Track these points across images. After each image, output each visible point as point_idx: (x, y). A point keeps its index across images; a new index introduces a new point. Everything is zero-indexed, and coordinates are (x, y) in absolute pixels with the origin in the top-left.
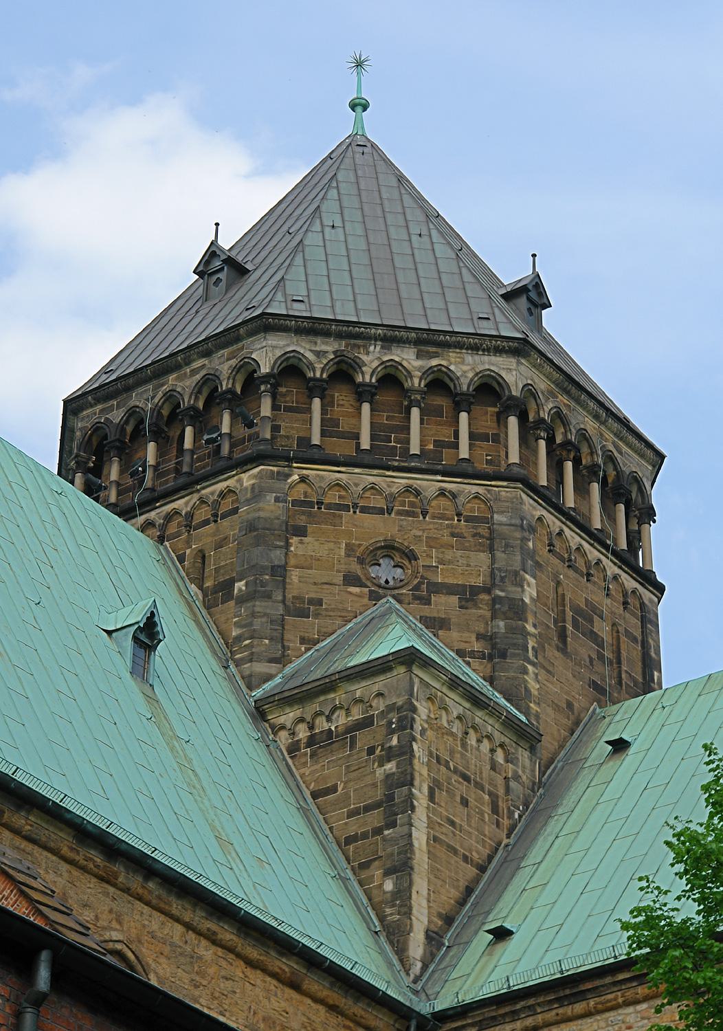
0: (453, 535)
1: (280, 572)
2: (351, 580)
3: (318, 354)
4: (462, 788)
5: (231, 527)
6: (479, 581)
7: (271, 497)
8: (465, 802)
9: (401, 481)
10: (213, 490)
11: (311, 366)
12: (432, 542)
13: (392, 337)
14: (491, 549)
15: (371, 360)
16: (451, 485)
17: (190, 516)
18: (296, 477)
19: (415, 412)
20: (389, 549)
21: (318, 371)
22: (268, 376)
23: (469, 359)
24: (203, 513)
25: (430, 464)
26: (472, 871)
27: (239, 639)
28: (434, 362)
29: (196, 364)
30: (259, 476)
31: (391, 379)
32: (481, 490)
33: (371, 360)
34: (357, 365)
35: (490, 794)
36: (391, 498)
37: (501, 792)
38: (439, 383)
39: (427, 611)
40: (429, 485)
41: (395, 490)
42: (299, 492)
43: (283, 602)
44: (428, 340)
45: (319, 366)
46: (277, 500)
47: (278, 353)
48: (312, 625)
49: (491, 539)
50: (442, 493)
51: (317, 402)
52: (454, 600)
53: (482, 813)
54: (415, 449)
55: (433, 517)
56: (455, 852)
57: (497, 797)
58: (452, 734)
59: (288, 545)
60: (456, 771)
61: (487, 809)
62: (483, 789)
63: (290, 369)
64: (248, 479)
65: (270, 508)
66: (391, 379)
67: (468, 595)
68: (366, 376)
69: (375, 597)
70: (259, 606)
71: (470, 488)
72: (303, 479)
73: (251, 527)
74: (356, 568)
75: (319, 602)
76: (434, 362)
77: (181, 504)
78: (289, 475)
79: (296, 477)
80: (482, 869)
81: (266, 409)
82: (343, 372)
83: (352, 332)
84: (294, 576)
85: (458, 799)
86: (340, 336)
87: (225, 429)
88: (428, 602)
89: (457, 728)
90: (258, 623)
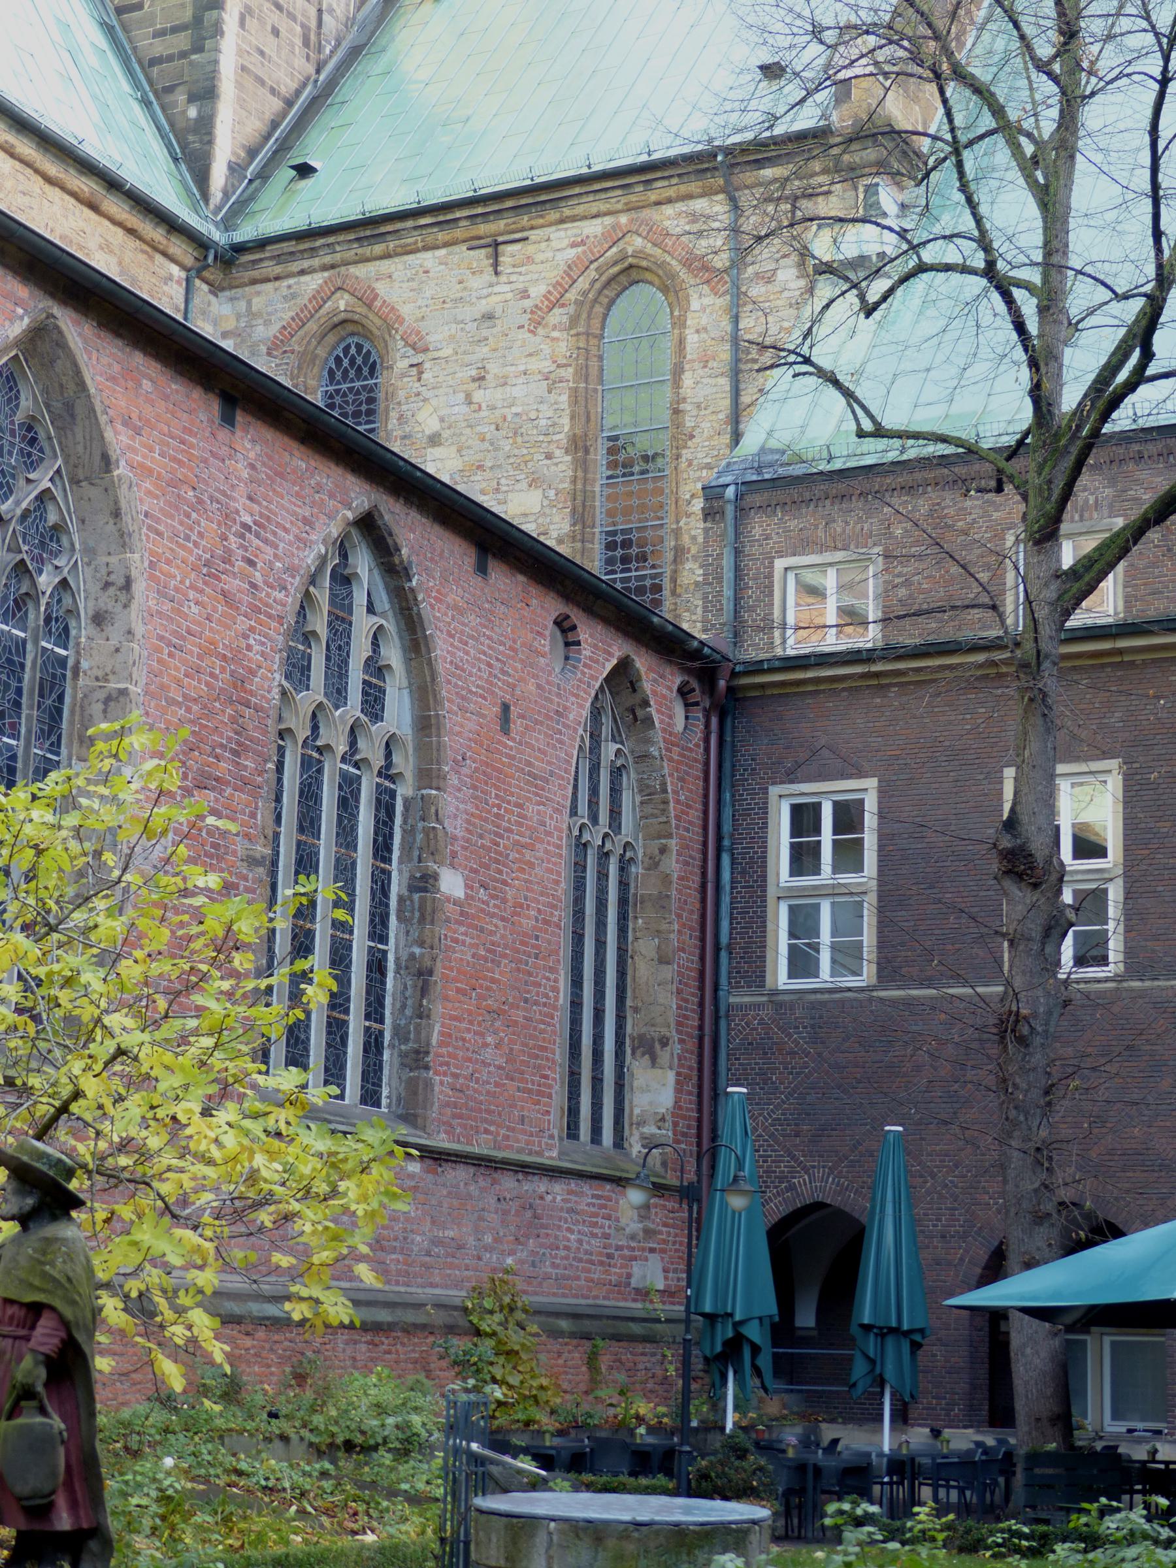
4: (274, 18)
8: (276, 32)
26: (277, 104)
35: (303, 26)
37: (313, 24)
53: (292, 45)
56: (262, 83)
57: (309, 29)
61: (298, 42)
62: (294, 19)
80: (289, 103)
85: (269, 28)
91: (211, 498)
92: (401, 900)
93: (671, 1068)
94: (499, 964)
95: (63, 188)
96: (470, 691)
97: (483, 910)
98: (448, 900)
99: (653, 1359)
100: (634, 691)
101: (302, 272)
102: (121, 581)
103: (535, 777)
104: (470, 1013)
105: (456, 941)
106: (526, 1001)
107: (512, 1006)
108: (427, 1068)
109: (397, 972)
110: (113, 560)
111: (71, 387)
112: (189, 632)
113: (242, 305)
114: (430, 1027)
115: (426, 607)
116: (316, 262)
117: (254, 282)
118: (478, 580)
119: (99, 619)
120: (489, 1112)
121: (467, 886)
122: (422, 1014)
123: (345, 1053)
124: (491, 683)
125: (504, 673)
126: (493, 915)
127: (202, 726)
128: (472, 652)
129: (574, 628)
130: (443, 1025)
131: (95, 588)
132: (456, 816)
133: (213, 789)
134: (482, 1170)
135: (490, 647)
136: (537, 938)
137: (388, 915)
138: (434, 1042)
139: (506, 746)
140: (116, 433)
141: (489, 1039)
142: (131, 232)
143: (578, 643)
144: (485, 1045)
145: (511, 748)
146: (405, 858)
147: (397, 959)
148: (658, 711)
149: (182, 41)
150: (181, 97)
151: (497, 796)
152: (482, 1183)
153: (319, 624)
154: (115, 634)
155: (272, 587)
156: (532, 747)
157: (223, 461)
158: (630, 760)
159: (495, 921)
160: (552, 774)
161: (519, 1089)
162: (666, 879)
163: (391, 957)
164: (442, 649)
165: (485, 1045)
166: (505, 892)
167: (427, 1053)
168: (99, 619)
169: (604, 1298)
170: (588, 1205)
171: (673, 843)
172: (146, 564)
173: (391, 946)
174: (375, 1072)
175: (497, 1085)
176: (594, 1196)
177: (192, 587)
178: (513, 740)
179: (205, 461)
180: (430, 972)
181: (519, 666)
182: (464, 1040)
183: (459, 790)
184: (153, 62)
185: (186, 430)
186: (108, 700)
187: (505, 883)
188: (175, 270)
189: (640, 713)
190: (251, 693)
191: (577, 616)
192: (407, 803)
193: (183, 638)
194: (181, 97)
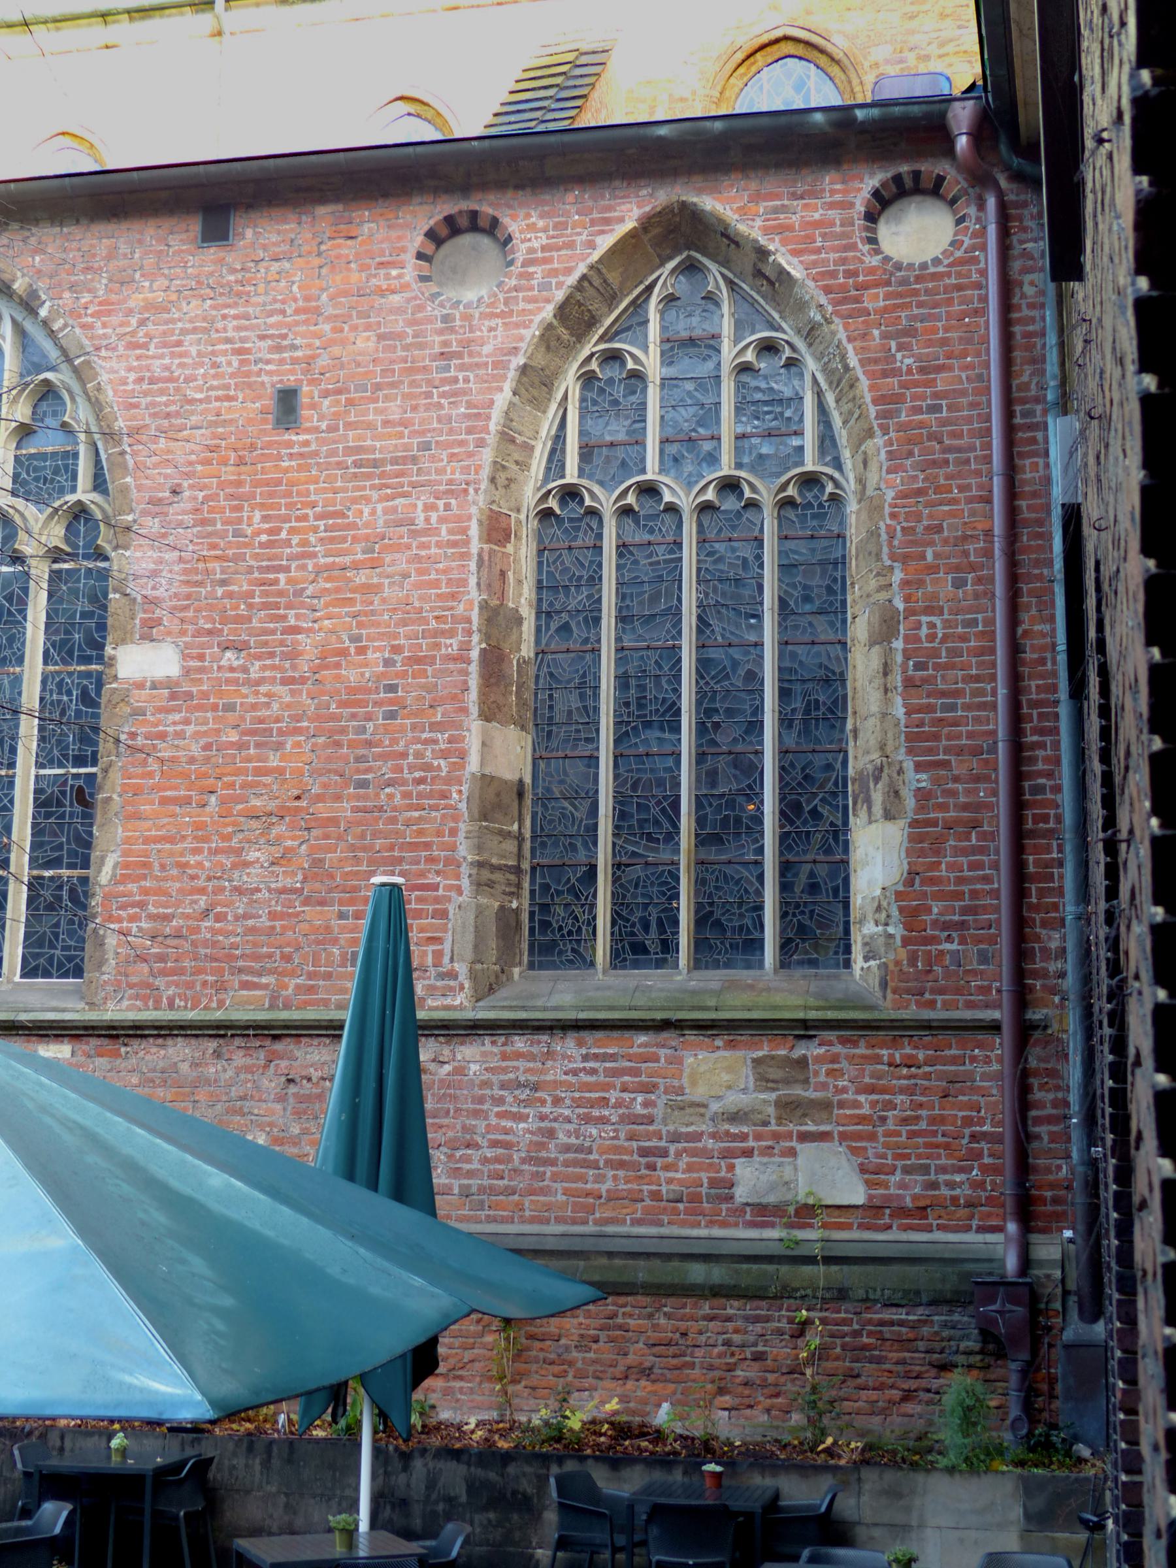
93: (889, 816)
94: (280, 746)
96: (191, 402)
97: (236, 682)
98: (140, 685)
99: (758, 1328)
100: (737, 244)
103: (375, 464)
104: (199, 826)
105: (162, 736)
106: (363, 784)
107: (320, 798)
118: (213, 252)
120: (256, 957)
121: (185, 657)
124: (248, 374)
125: (279, 349)
126: (259, 682)
128: (193, 350)
129: (495, 222)
130: (125, 854)
134: (238, 1041)
135: (238, 329)
136: (392, 688)
139: (290, 444)
141: (253, 855)
144: (247, 864)
145: (306, 443)
151: (265, 518)
152: (239, 1059)
156: (370, 426)
159: (263, 689)
160: (425, 446)
161: (342, 916)
165: (247, 864)
166: (296, 643)
169: (637, 1222)
170: (575, 1072)
175: (273, 916)
176: (585, 1058)
178: (308, 431)
181: (327, 327)
187: (296, 630)
189: (768, 271)
191: (486, 205)
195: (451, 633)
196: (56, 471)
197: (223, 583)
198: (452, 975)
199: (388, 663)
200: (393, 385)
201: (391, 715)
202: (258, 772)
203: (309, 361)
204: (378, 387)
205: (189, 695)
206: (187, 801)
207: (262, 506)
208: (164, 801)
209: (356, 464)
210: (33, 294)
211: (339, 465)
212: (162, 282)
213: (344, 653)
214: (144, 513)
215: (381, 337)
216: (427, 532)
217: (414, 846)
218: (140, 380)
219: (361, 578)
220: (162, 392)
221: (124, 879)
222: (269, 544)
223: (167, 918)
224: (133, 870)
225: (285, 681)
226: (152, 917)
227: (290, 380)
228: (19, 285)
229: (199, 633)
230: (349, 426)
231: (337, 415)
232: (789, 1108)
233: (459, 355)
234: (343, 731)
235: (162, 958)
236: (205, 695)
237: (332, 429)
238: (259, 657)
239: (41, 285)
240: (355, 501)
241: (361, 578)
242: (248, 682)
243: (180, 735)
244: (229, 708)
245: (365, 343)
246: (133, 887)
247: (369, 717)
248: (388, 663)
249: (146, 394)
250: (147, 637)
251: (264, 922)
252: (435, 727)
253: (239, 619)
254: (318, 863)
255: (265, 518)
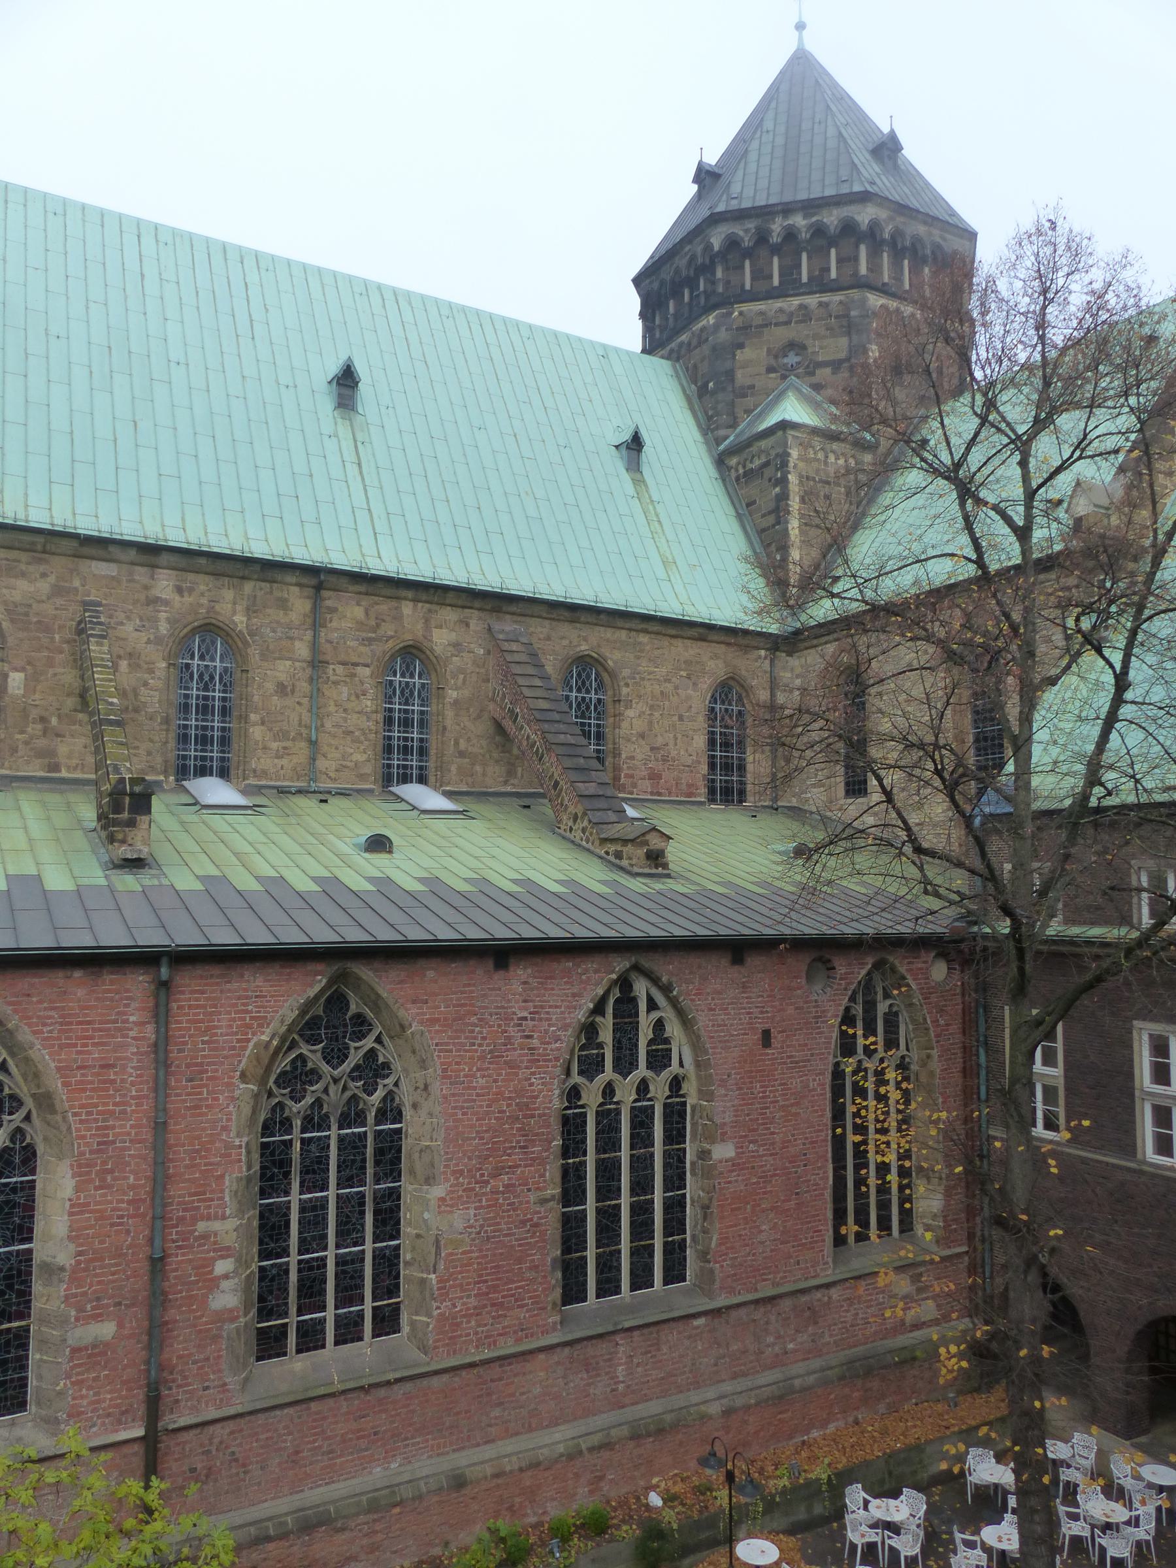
0: (827, 329)
1: (730, 375)
2: (771, 369)
3: (746, 231)
5: (706, 349)
6: (843, 355)
7: (723, 329)
9: (796, 302)
10: (697, 327)
11: (742, 239)
12: (816, 337)
13: (787, 209)
14: (849, 334)
15: (777, 227)
16: (825, 298)
17: (689, 344)
18: (736, 313)
19: (804, 256)
20: (794, 346)
21: (747, 242)
22: (719, 252)
23: (835, 212)
24: (695, 342)
25: (820, 284)
27: (712, 417)
28: (814, 219)
29: (687, 249)
30: (716, 317)
31: (790, 235)
32: (842, 298)
33: (777, 227)
34: (770, 232)
36: (791, 314)
38: (819, 231)
39: (814, 380)
40: (812, 301)
41: (793, 308)
42: (739, 323)
43: (733, 391)
44: (810, 206)
45: (746, 239)
46: (727, 330)
47: (723, 236)
48: (749, 401)
49: (849, 326)
50: (821, 304)
51: (747, 263)
52: (828, 370)
54: (805, 279)
55: (816, 320)
58: (818, 460)
59: (734, 355)
60: (821, 481)
63: (732, 243)
64: (711, 319)
65: (723, 335)
66: (790, 235)
67: (836, 365)
68: (775, 238)
69: (784, 377)
70: (720, 396)
71: (836, 298)
72: (741, 313)
73: (714, 349)
74: (773, 362)
75: (752, 387)
76: (814, 219)
77: (684, 337)
78: (732, 313)
79: (736, 313)
81: (719, 274)
82: (762, 238)
83: (765, 212)
84: (739, 374)
86: (757, 216)
87: (702, 288)
88: (813, 374)
89: (820, 455)
90: (720, 406)
91: (491, 1015)
92: (693, 1164)
95: (683, 637)
97: (753, 1157)
98: (721, 1162)
101: (826, 643)
102: (422, 1086)
103: (797, 1062)
105: (730, 1182)
106: (797, 1194)
108: (709, 1262)
109: (692, 1204)
110: (417, 1075)
111: (373, 997)
112: (478, 1095)
113: (803, 660)
114: (711, 1239)
115: (684, 1002)
116: (831, 637)
117: (807, 648)
119: (415, 1106)
121: (737, 1148)
122: (705, 1231)
123: (653, 1263)
125: (762, 1012)
127: (494, 1143)
131: (411, 1089)
132: (724, 1112)
133: (507, 1173)
136: (805, 1154)
137: (684, 1173)
138: (713, 1245)
139: (768, 1054)
140: (407, 1010)
141: (764, 1227)
142: (728, 644)
143: (834, 968)
146: (692, 1141)
147: (691, 1198)
148: (914, 980)
149: (771, 519)
150: (773, 548)
153: (606, 1036)
154: (423, 1113)
155: (548, 1043)
157: (500, 989)
158: (902, 1007)
162: (932, 1074)
163: (688, 1196)
164: (703, 1021)
167: (708, 1253)
168: (415, 1106)
171: (935, 1053)
172: (439, 1072)
173: (688, 1191)
174: (680, 1264)
175: (772, 1251)
177: (478, 1070)
179: (484, 996)
180: (708, 1208)
182: (740, 1236)
183: (726, 1095)
184: (763, 530)
185: (465, 985)
186: (421, 1151)
187: (773, 1133)
188: (763, 653)
190: (535, 1109)
192: (694, 1108)
193: (474, 1101)
194: (773, 548)
195: (821, 1131)
196: (663, 1057)
197: (748, 1115)
198: (827, 1263)
199: (804, 1144)
200: (801, 1029)
201: (805, 1165)
202: (765, 1193)
203: (773, 1018)
204: (796, 1030)
205: (739, 1164)
206: (739, 1208)
207: (760, 1081)
208: (732, 1210)
209: (791, 1063)
210: (670, 984)
211: (785, 1063)
212: (718, 980)
213: (790, 1141)
214: (719, 1086)
215: (797, 1008)
216: (814, 1090)
217: (814, 1216)
218: (713, 1026)
219: (793, 1110)
220: (722, 1031)
221: (720, 1244)
222: (763, 1097)
223: (736, 1258)
224: (723, 1241)
225: (771, 1155)
226: (732, 1259)
227: (766, 1026)
228: (664, 979)
229: (741, 1137)
230: (788, 1046)
231: (783, 1042)
232: (920, 1290)
233: (820, 1017)
234: (790, 1173)
235: (735, 1275)
236: (744, 1163)
237: (782, 1048)
238: (762, 1145)
239: (674, 979)
240: (791, 1078)
241: (793, 1110)
242: (760, 1156)
243: (736, 1181)
244: (753, 1168)
245: (790, 1010)
246: (723, 1248)
247: (799, 1166)
248: (804, 1144)
249: (716, 1031)
250: (723, 1141)
251: (769, 1254)
252: (819, 1168)
253: (754, 1130)
254: (785, 1227)
255: (762, 1087)
